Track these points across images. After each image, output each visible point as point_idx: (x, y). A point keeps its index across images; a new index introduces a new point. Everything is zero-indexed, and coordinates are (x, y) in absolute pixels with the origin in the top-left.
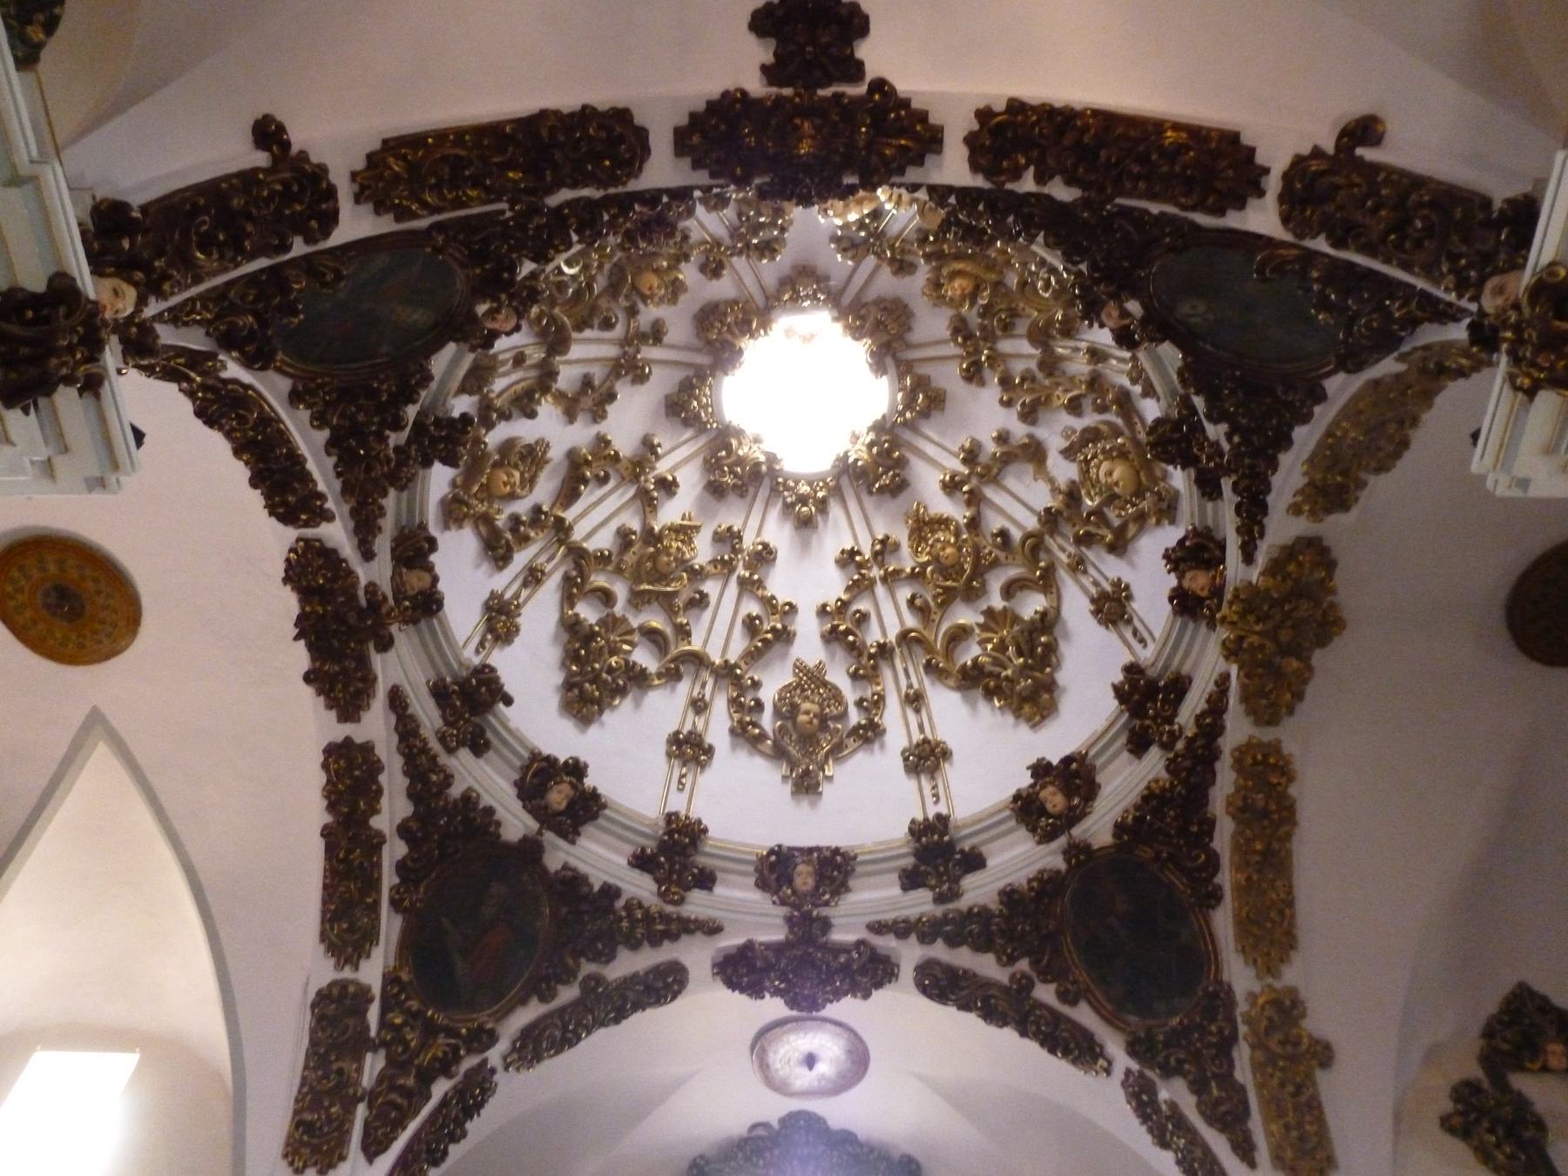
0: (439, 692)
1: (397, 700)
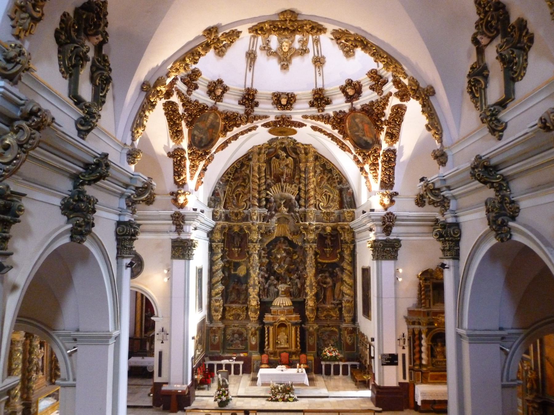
0: (312, 105)
1: (305, 117)
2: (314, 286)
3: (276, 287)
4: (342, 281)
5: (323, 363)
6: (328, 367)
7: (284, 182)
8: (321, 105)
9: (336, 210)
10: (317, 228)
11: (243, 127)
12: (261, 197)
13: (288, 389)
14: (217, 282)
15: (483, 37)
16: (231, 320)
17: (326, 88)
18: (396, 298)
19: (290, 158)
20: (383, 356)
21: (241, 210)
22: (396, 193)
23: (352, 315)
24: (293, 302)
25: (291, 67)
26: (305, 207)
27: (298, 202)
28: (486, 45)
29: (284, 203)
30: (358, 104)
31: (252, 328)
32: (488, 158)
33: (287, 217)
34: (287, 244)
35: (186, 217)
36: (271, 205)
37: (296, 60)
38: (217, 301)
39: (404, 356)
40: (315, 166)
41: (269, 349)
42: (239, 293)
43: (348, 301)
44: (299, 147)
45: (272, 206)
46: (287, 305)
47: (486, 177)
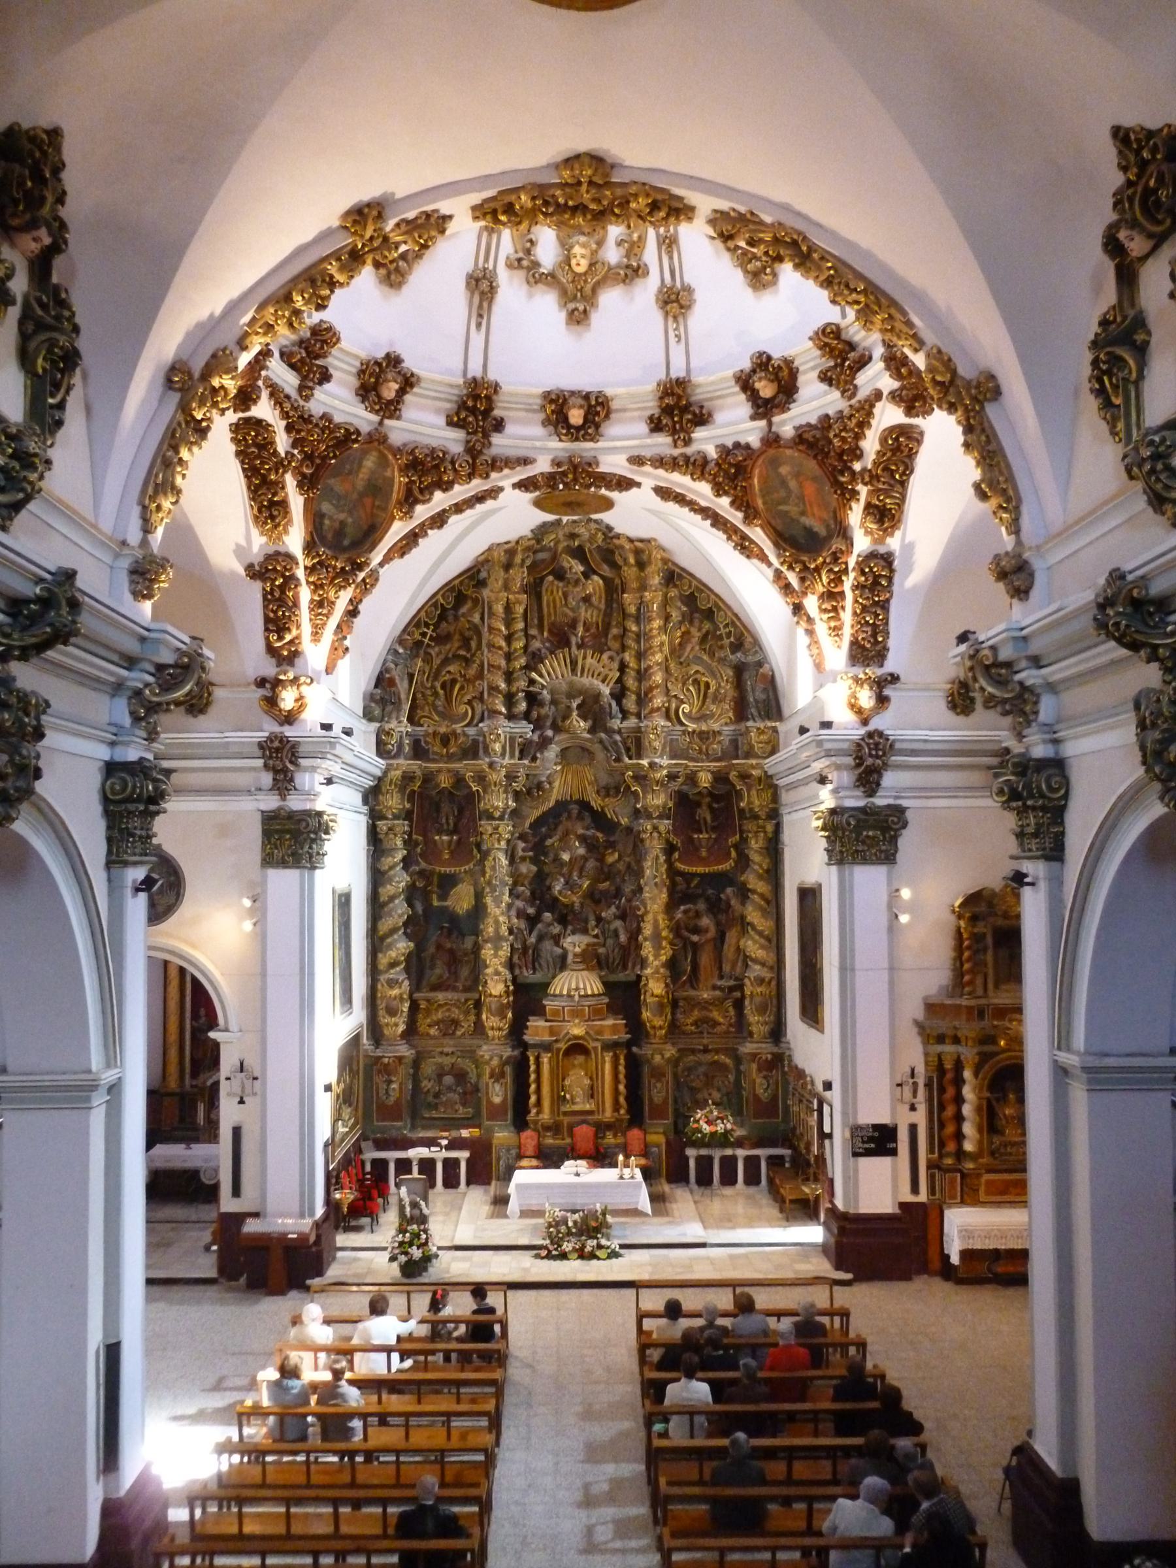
0: (656, 426)
1: (637, 461)
2: (665, 938)
3: (557, 943)
4: (744, 925)
5: (691, 1153)
6: (705, 1164)
7: (579, 647)
8: (681, 427)
9: (726, 724)
10: (672, 777)
11: (460, 492)
12: (514, 689)
13: (594, 1224)
14: (393, 931)
15: (1134, 233)
16: (433, 1038)
17: (697, 379)
18: (892, 969)
19: (596, 578)
20: (856, 1130)
21: (458, 727)
22: (892, 675)
23: (772, 1018)
24: (605, 984)
25: (595, 317)
26: (638, 716)
27: (619, 704)
28: (1144, 259)
29: (579, 707)
30: (787, 424)
31: (491, 1058)
32: (1143, 577)
33: (588, 745)
34: (588, 820)
35: (302, 749)
36: (543, 711)
37: (610, 299)
38: (392, 983)
39: (913, 1128)
40: (665, 603)
41: (541, 1116)
42: (454, 961)
43: (761, 981)
44: (622, 547)
45: (547, 716)
46: (589, 992)
47: (1137, 631)
